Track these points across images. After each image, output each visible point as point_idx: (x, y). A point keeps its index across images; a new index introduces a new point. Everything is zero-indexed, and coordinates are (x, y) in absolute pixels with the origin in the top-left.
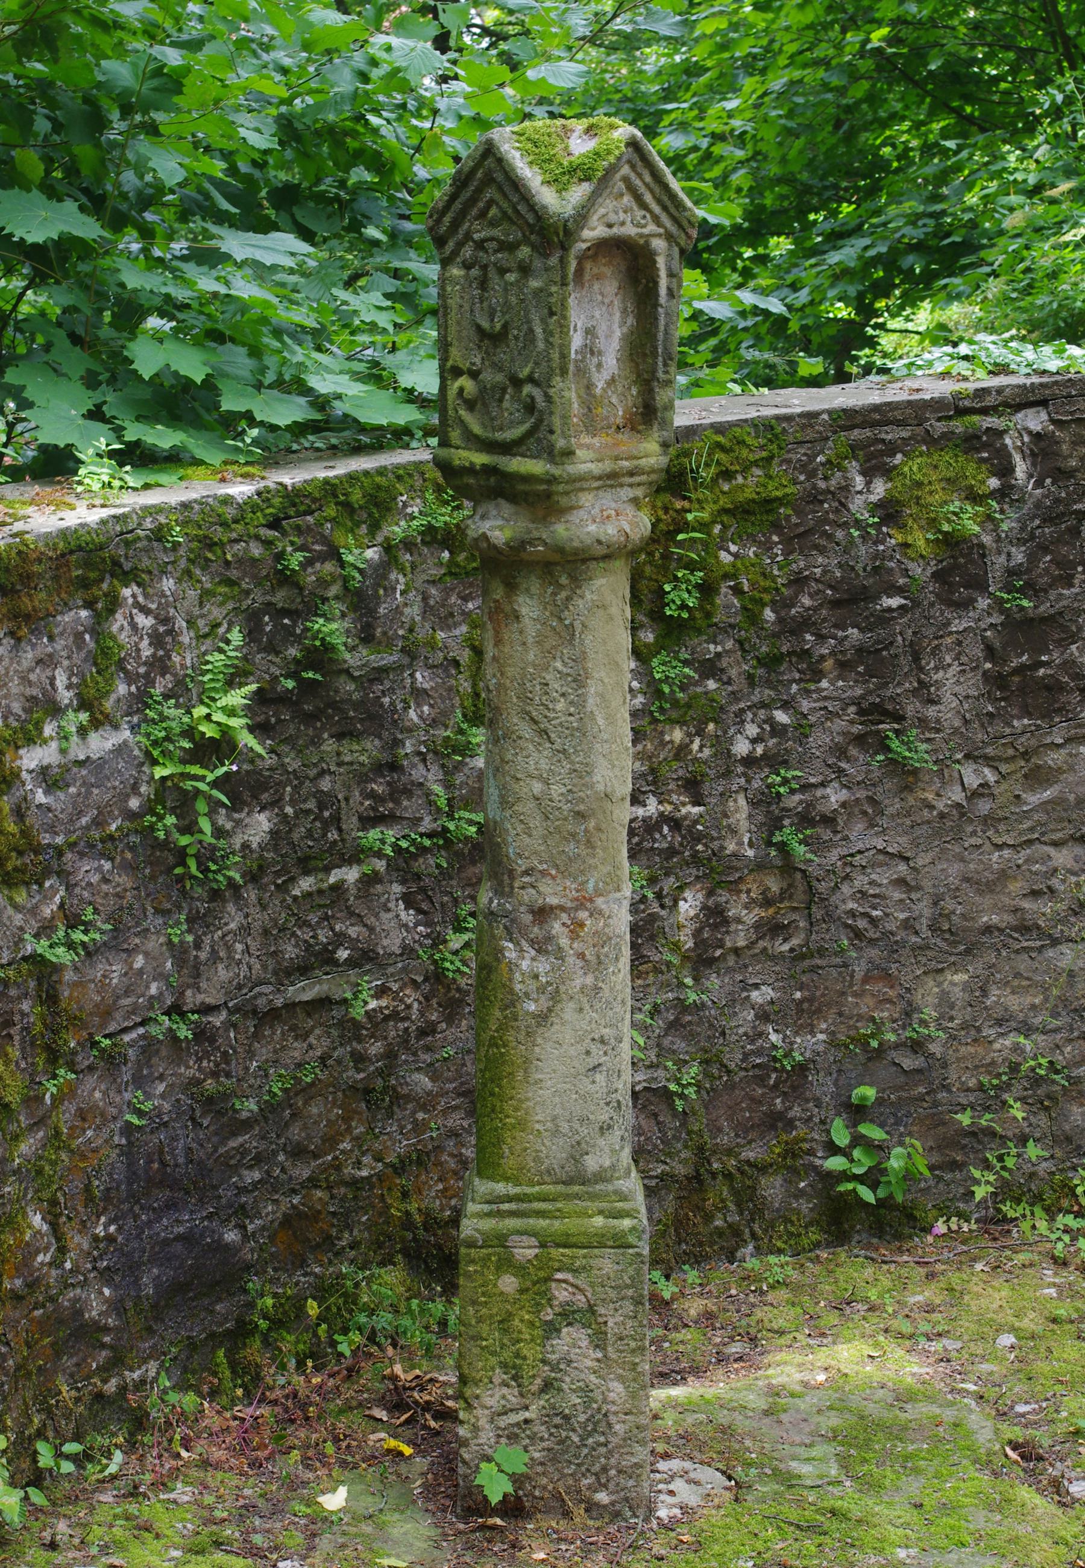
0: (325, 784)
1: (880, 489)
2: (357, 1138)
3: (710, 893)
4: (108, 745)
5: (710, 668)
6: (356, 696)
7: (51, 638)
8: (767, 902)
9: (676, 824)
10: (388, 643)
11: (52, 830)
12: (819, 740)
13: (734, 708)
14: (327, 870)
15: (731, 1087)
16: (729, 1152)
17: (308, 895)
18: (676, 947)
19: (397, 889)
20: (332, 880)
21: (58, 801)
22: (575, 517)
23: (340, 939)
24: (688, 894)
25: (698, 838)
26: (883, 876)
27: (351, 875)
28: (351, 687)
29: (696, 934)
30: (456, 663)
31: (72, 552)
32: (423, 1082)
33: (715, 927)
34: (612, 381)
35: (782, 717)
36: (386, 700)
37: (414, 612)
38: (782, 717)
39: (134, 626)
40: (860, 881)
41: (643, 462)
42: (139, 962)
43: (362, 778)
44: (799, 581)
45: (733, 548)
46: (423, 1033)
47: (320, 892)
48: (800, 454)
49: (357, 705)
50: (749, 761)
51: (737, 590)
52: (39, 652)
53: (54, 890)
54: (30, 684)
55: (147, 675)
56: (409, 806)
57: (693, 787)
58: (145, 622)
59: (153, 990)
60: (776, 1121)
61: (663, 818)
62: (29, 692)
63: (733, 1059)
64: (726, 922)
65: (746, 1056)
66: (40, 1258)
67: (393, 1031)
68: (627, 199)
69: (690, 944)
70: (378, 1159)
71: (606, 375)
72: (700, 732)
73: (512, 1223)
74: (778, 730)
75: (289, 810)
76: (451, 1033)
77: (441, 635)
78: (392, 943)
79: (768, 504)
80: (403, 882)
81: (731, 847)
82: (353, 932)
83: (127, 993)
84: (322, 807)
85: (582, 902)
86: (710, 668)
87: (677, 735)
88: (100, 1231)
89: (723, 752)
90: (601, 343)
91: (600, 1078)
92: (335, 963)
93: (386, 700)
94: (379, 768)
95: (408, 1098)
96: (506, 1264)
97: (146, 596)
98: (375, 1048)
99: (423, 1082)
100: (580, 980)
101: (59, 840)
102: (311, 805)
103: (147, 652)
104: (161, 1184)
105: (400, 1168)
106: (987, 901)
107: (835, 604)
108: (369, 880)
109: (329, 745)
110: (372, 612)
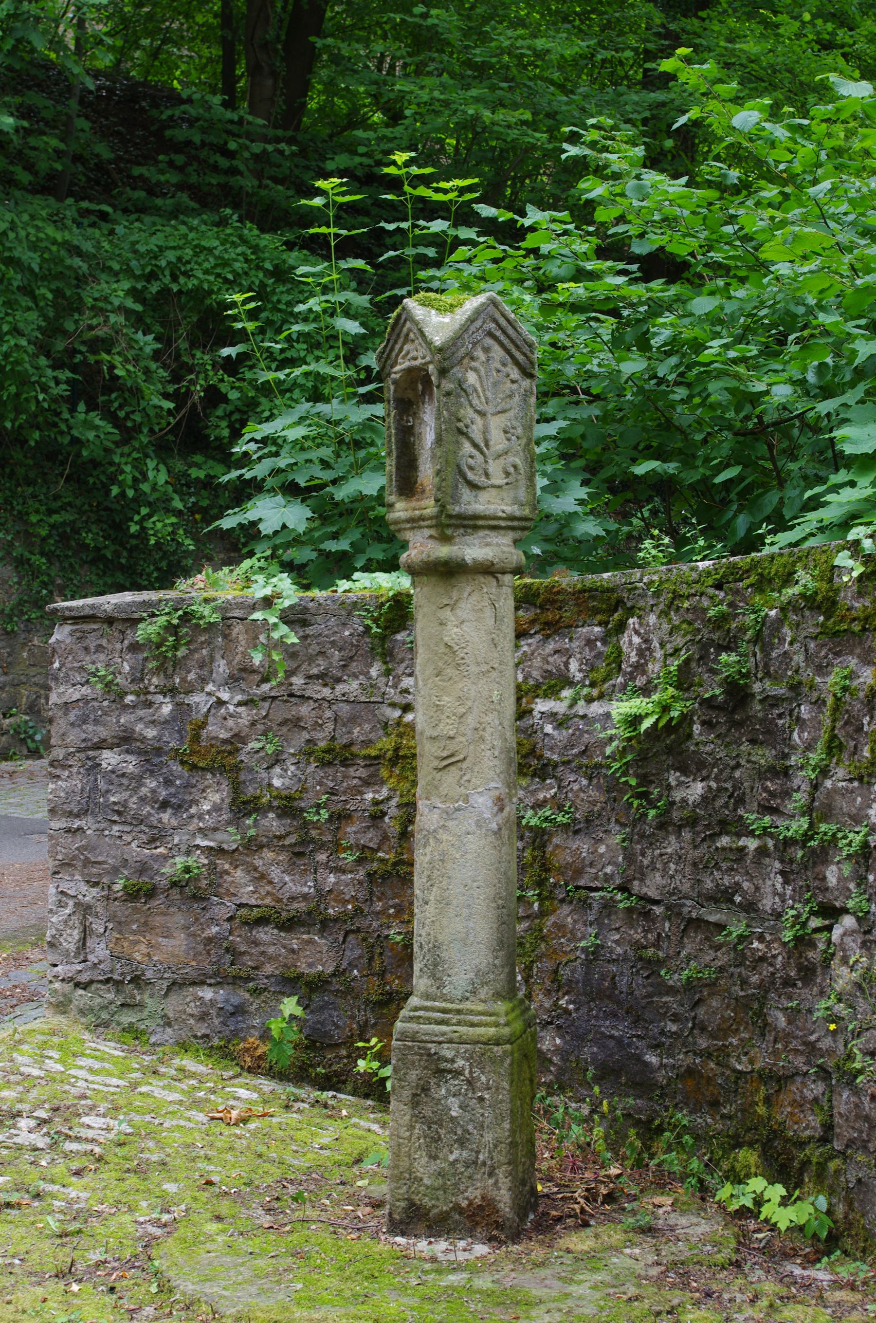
0: (737, 774)
2: (741, 1040)
4: (601, 711)
7: (571, 640)
17: (724, 849)
19: (777, 865)
20: (741, 843)
27: (752, 844)
31: (585, 591)
32: (782, 1021)
37: (799, 659)
39: (630, 641)
41: (425, 512)
42: (602, 849)
47: (731, 849)
52: (558, 646)
54: (548, 663)
55: (631, 673)
58: (636, 640)
59: (609, 870)
62: (546, 667)
75: (714, 785)
77: (818, 679)
80: (782, 861)
83: (591, 865)
92: (732, 902)
97: (641, 624)
101: (555, 757)
102: (728, 785)
103: (634, 659)
104: (609, 997)
108: (762, 851)
109: (745, 747)
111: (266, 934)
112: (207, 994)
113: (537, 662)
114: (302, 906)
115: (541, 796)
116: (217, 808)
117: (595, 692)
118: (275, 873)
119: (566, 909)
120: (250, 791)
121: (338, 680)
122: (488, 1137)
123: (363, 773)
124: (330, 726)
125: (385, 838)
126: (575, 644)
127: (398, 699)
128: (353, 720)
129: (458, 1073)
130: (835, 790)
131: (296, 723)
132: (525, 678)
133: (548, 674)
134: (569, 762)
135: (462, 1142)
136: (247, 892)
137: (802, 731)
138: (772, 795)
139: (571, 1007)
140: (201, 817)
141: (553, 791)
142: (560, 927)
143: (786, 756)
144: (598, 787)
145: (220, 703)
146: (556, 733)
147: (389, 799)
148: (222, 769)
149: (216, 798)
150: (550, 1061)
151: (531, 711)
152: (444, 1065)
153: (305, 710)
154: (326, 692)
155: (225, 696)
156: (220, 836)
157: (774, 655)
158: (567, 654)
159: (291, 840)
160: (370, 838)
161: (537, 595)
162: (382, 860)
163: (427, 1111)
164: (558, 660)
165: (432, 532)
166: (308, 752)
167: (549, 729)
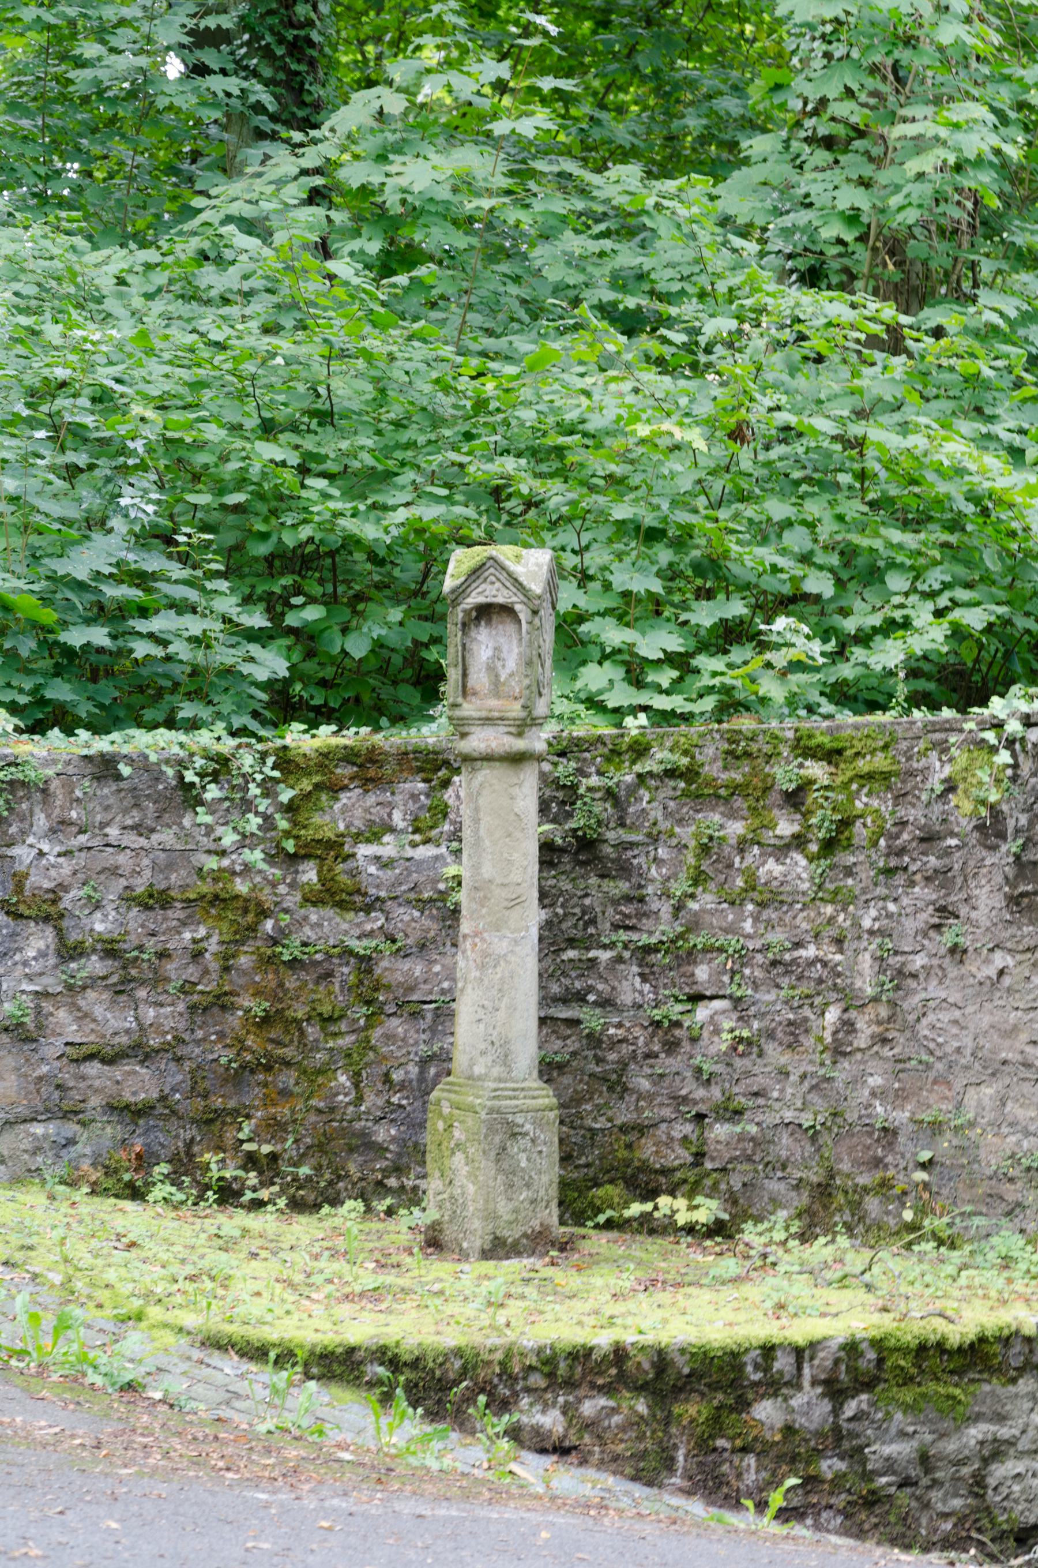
0: (587, 901)
1: (947, 771)
3: (846, 1010)
5: (849, 872)
6: (613, 856)
7: (393, 794)
8: (879, 1023)
9: (825, 964)
10: (633, 828)
11: (378, 887)
12: (911, 925)
13: (864, 898)
14: (588, 949)
15: (850, 1134)
16: (848, 1176)
17: (571, 960)
18: (820, 1039)
19: (635, 969)
21: (387, 875)
22: (471, 738)
23: (590, 989)
24: (832, 1008)
25: (839, 975)
26: (945, 1017)
27: (605, 956)
28: (610, 850)
29: (835, 1033)
30: (686, 847)
32: (645, 1085)
33: (849, 1032)
34: (512, 675)
35: (892, 907)
36: (635, 862)
37: (657, 814)
38: (892, 907)
40: (931, 1017)
42: (437, 968)
43: (615, 902)
44: (903, 824)
45: (865, 799)
46: (648, 1056)
48: (904, 745)
49: (613, 861)
50: (871, 932)
51: (865, 825)
52: (380, 799)
53: (378, 919)
56: (646, 923)
57: (839, 942)
60: (877, 1163)
61: (817, 960)
63: (852, 1116)
64: (855, 1031)
65: (860, 1117)
66: (341, 1097)
67: (625, 1049)
68: (498, 585)
69: (829, 1040)
70: (610, 1120)
71: (508, 671)
72: (844, 910)
73: (445, 1095)
74: (889, 916)
75: (560, 911)
76: (670, 1061)
77: (677, 830)
78: (626, 997)
79: (886, 776)
80: (640, 966)
81: (858, 984)
82: (600, 987)
83: (425, 982)
84: (584, 913)
85: (476, 934)
86: (849, 872)
87: (829, 910)
88: (395, 1100)
89: (856, 924)
90: (504, 655)
91: (482, 1026)
93: (635, 862)
94: (628, 899)
95: (633, 1091)
96: (440, 1115)
98: (612, 1056)
99: (645, 1085)
100: (475, 973)
101: (383, 894)
102: (577, 910)
105: (624, 1129)
106: (1007, 1043)
107: (922, 840)
109: (593, 880)
110: (624, 810)
111: (93, 1068)
112: (38, 1129)
113: (359, 812)
114: (124, 1040)
115: (368, 927)
116: (42, 955)
117: (417, 838)
118: (98, 1011)
119: (395, 1022)
120: (74, 937)
121: (153, 830)
122: (545, 1179)
123: (180, 914)
124: (148, 873)
125: (206, 972)
126: (398, 798)
127: (212, 846)
128: (170, 866)
129: (526, 1134)
130: (703, 911)
131: (114, 871)
132: (347, 827)
133: (371, 823)
134: (395, 898)
135: (528, 1186)
136: (72, 1031)
137: (659, 867)
138: (627, 916)
139: (404, 1102)
140: (25, 963)
141: (379, 923)
142: (390, 1038)
143: (640, 887)
144: (432, 917)
145: (41, 854)
146: (380, 873)
147: (208, 937)
148: (47, 919)
149: (41, 944)
150: (387, 1149)
151: (354, 855)
152: (517, 1130)
153: (123, 859)
154: (142, 842)
155: (46, 847)
156: (47, 980)
157: (631, 810)
158: (392, 806)
159: (114, 979)
160: (192, 972)
161: (357, 755)
162: (202, 993)
163: (505, 1166)
164: (384, 812)
165: (513, 730)
166: (129, 898)
167: (372, 869)
